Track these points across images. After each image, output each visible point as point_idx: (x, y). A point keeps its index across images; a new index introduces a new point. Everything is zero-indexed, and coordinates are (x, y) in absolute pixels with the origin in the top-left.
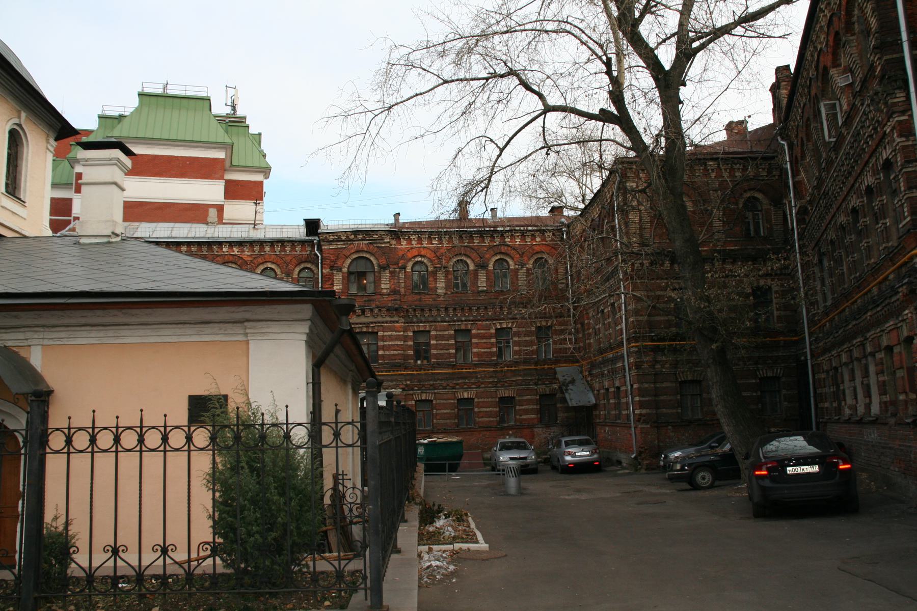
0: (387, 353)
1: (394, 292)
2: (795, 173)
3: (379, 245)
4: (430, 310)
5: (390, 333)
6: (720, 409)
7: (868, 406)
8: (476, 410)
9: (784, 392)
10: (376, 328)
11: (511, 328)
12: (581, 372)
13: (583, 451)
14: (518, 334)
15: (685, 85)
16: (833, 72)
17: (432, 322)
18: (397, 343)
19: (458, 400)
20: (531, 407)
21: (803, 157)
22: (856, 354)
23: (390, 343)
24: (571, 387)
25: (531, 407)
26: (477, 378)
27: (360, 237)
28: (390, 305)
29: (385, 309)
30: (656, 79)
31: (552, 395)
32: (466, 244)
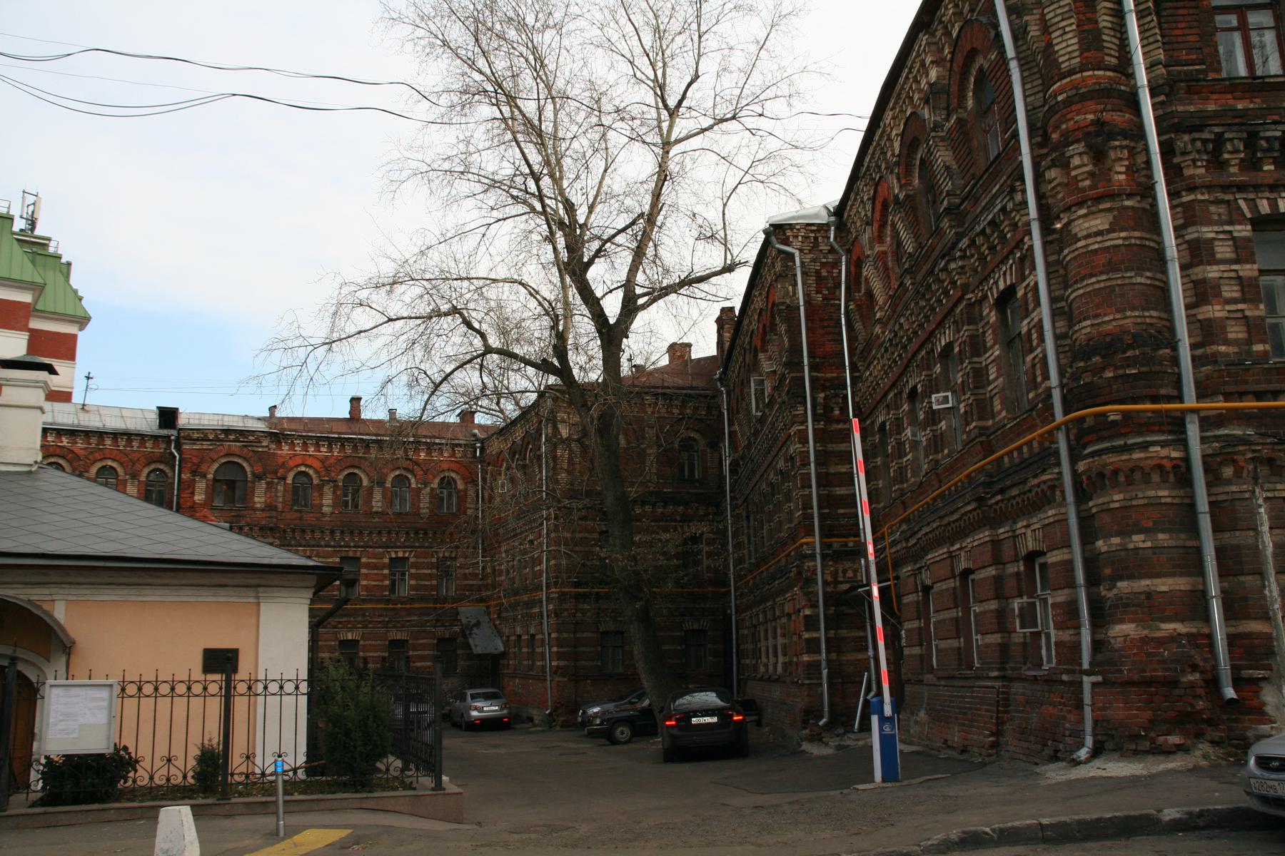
1: (270, 507)
2: (731, 423)
3: (255, 449)
4: (313, 532)
6: (640, 665)
7: (775, 665)
8: (361, 654)
9: (709, 646)
11: (408, 558)
12: (489, 614)
13: (491, 705)
14: (415, 565)
15: (627, 337)
16: (761, 356)
17: (313, 546)
19: (340, 641)
20: (426, 653)
21: (738, 412)
22: (769, 615)
24: (475, 630)
25: (426, 653)
26: (364, 615)
27: (232, 437)
28: (263, 523)
30: (599, 331)
31: (452, 639)
32: (361, 455)
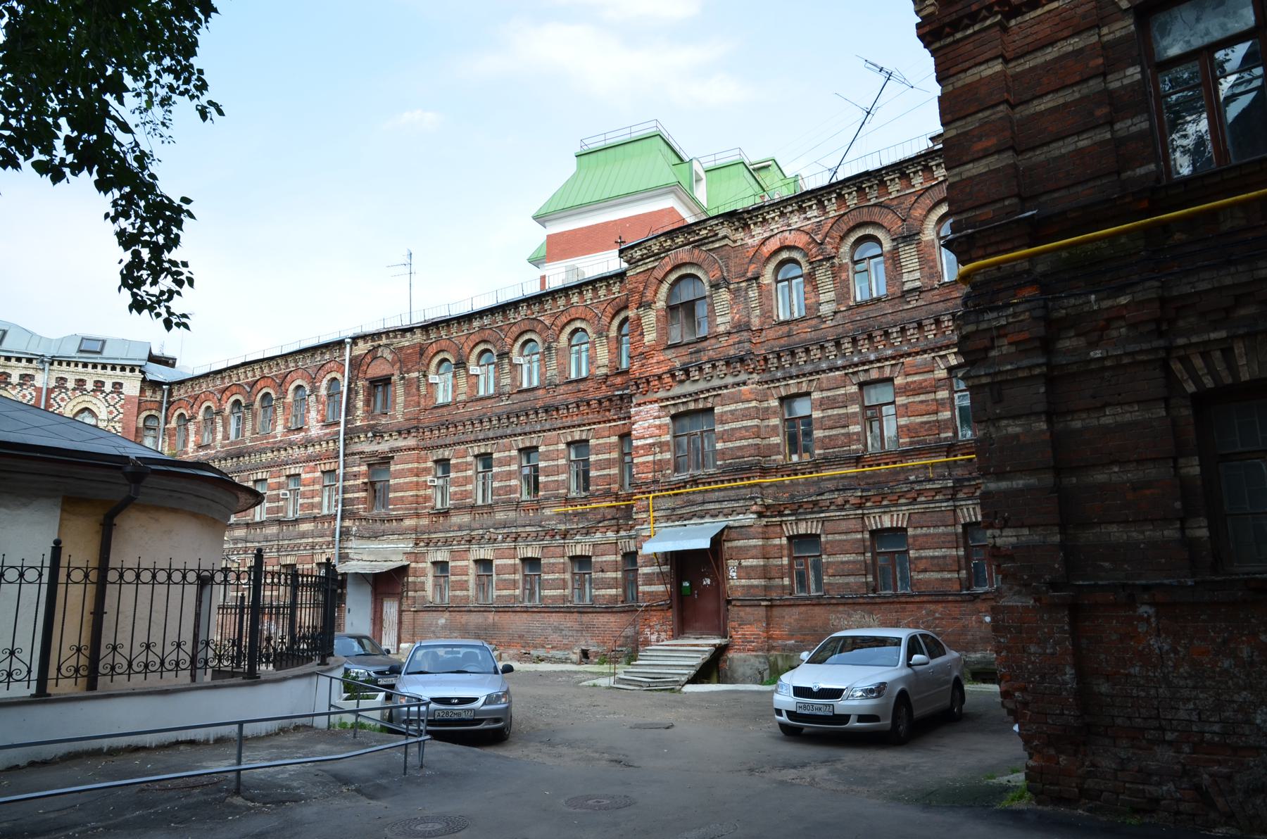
0: (730, 445)
1: (742, 327)
3: (711, 246)
4: (807, 351)
5: (733, 407)
10: (710, 400)
17: (811, 374)
18: (745, 423)
19: (872, 533)
23: (734, 425)
26: (907, 481)
27: (680, 240)
28: (732, 352)
29: (721, 363)
32: (873, 202)
